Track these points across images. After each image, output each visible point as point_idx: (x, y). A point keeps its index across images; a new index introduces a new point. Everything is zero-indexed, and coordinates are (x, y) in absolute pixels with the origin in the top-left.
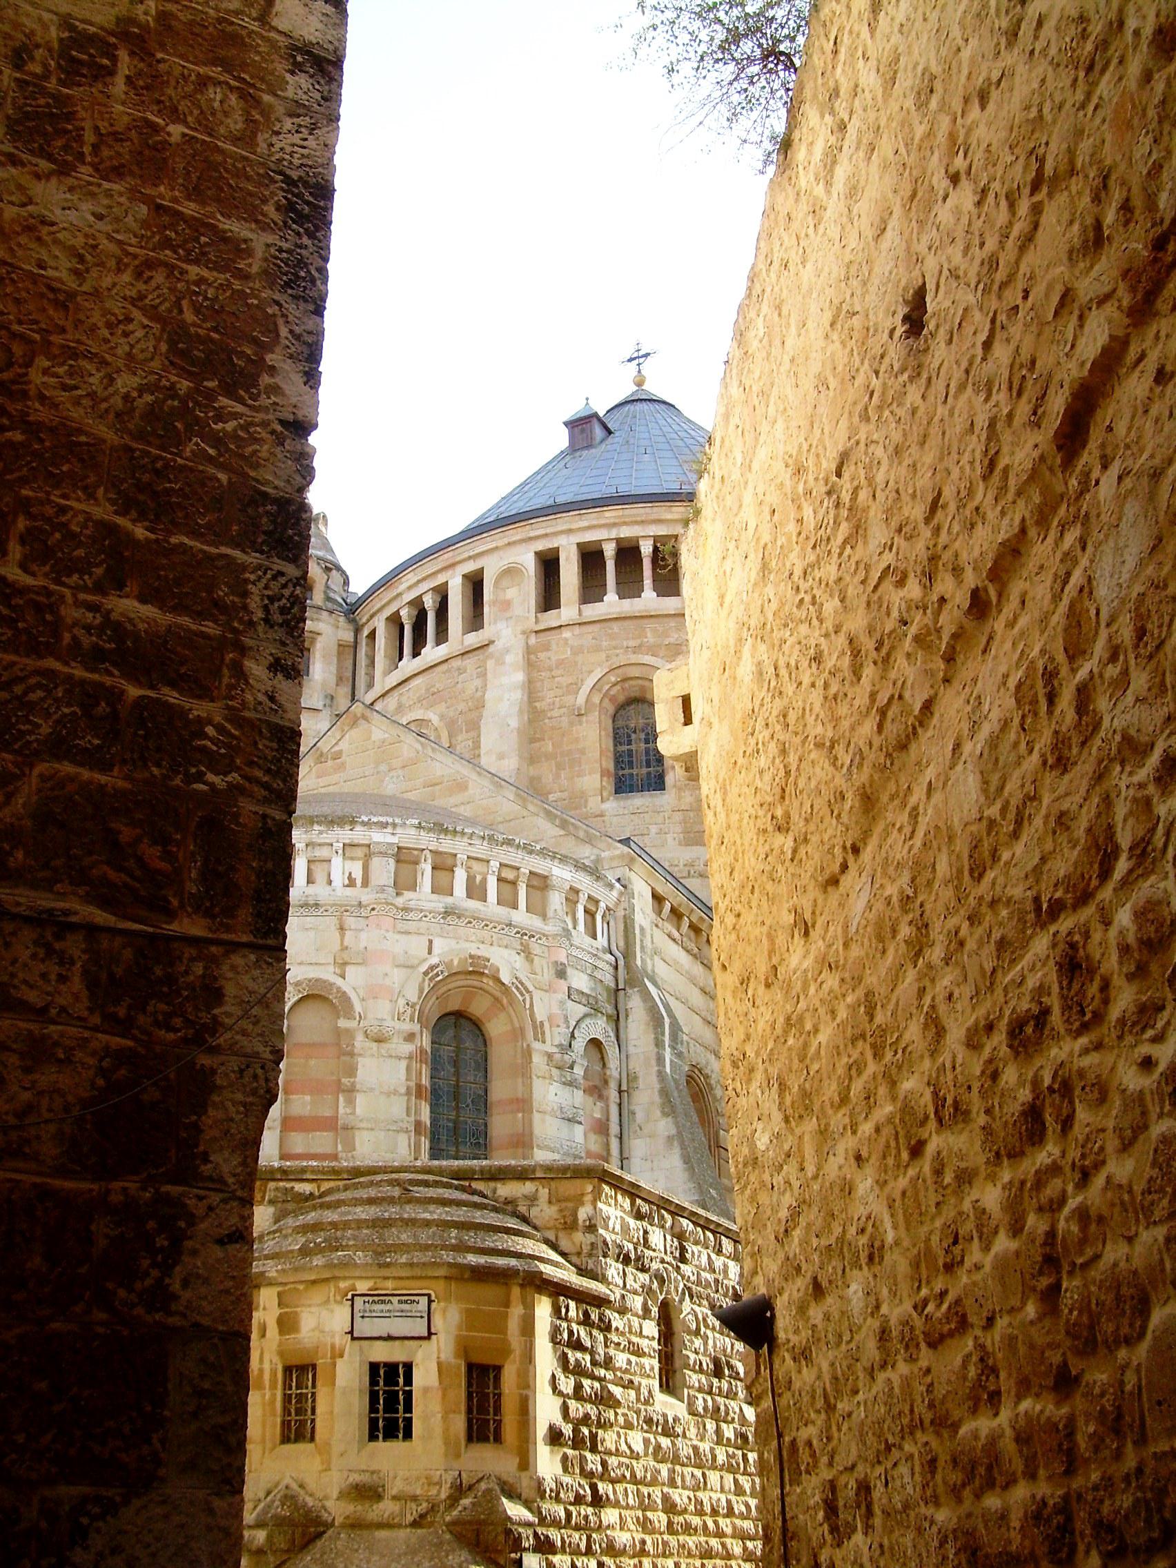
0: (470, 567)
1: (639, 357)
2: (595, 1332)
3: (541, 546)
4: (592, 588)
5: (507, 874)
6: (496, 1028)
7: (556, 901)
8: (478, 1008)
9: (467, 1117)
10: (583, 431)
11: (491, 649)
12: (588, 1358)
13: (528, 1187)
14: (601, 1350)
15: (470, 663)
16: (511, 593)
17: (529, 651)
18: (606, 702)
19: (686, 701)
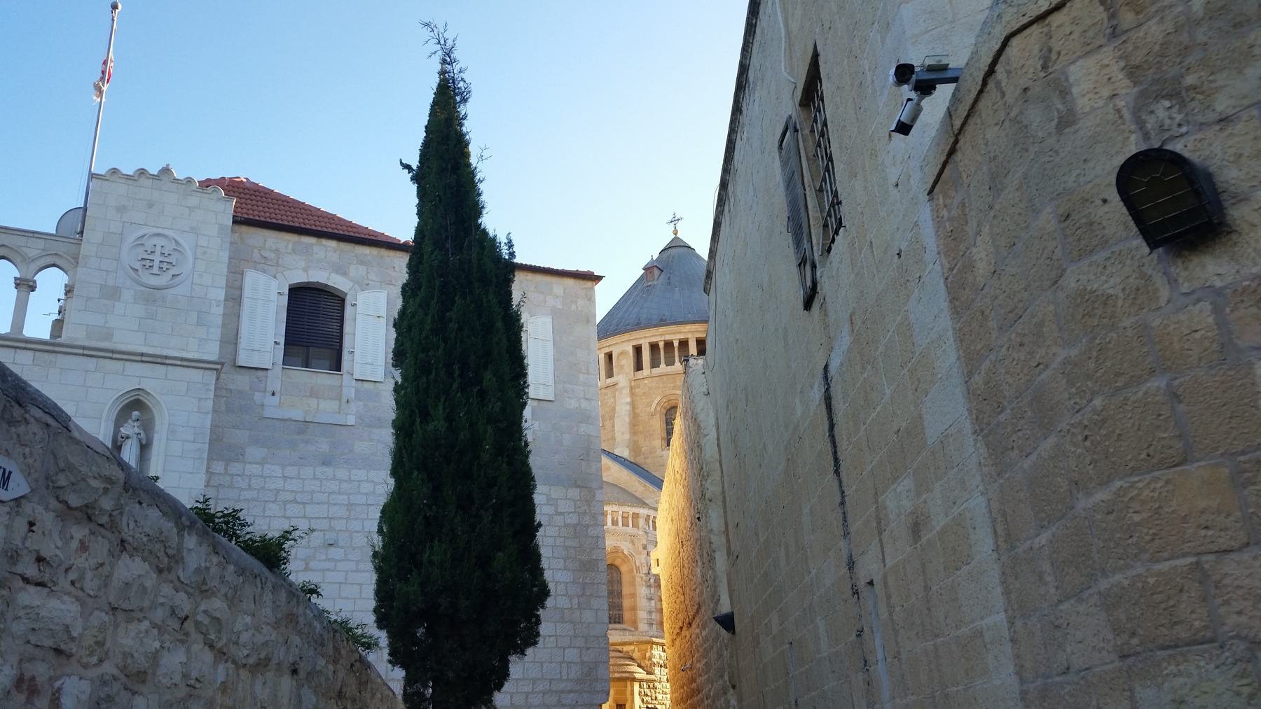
0: (607, 350)
1: (675, 220)
2: (652, 690)
3: (635, 343)
4: (655, 364)
5: (625, 515)
6: (624, 569)
7: (641, 522)
8: (617, 562)
9: (616, 587)
10: (650, 273)
11: (617, 387)
12: (650, 698)
13: (632, 647)
14: (654, 695)
15: (609, 391)
16: (624, 362)
17: (632, 388)
18: (662, 410)
19: (658, 560)
